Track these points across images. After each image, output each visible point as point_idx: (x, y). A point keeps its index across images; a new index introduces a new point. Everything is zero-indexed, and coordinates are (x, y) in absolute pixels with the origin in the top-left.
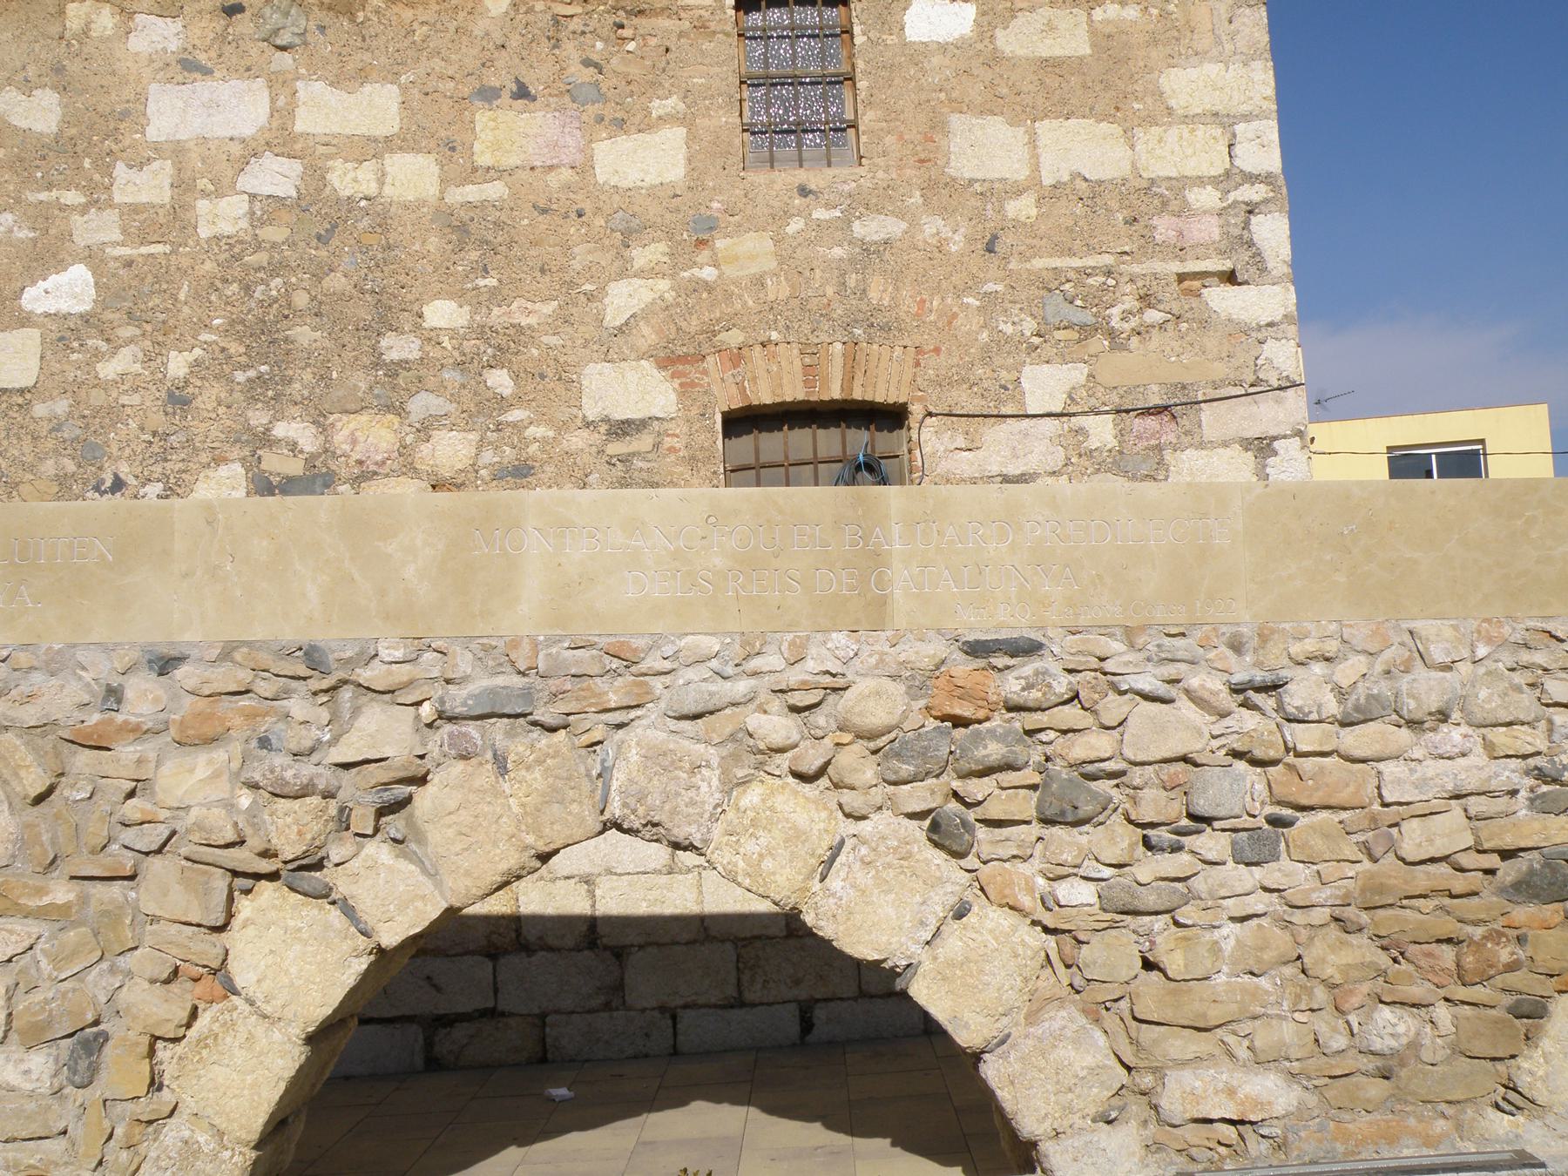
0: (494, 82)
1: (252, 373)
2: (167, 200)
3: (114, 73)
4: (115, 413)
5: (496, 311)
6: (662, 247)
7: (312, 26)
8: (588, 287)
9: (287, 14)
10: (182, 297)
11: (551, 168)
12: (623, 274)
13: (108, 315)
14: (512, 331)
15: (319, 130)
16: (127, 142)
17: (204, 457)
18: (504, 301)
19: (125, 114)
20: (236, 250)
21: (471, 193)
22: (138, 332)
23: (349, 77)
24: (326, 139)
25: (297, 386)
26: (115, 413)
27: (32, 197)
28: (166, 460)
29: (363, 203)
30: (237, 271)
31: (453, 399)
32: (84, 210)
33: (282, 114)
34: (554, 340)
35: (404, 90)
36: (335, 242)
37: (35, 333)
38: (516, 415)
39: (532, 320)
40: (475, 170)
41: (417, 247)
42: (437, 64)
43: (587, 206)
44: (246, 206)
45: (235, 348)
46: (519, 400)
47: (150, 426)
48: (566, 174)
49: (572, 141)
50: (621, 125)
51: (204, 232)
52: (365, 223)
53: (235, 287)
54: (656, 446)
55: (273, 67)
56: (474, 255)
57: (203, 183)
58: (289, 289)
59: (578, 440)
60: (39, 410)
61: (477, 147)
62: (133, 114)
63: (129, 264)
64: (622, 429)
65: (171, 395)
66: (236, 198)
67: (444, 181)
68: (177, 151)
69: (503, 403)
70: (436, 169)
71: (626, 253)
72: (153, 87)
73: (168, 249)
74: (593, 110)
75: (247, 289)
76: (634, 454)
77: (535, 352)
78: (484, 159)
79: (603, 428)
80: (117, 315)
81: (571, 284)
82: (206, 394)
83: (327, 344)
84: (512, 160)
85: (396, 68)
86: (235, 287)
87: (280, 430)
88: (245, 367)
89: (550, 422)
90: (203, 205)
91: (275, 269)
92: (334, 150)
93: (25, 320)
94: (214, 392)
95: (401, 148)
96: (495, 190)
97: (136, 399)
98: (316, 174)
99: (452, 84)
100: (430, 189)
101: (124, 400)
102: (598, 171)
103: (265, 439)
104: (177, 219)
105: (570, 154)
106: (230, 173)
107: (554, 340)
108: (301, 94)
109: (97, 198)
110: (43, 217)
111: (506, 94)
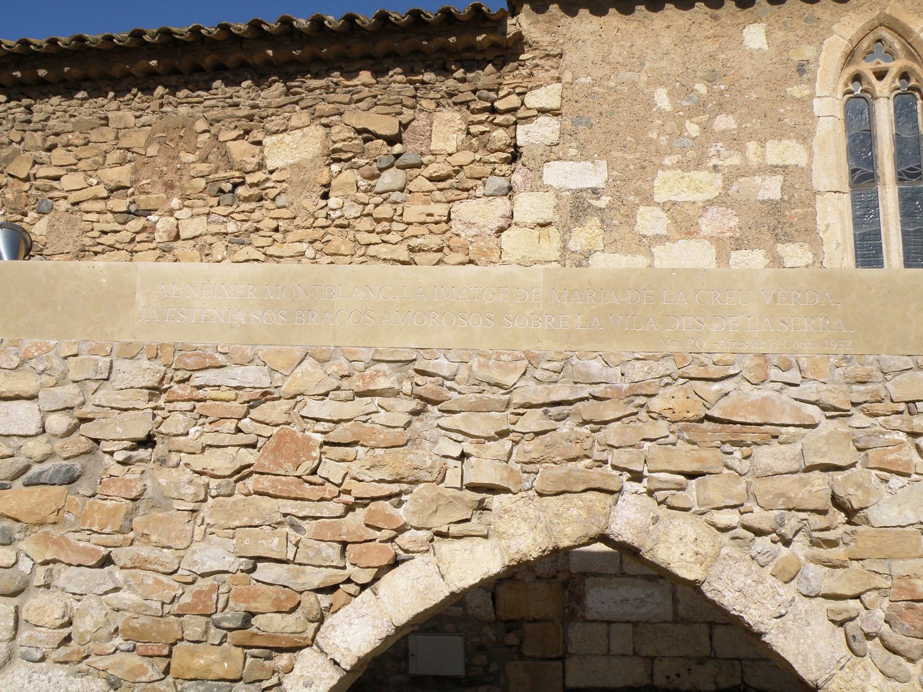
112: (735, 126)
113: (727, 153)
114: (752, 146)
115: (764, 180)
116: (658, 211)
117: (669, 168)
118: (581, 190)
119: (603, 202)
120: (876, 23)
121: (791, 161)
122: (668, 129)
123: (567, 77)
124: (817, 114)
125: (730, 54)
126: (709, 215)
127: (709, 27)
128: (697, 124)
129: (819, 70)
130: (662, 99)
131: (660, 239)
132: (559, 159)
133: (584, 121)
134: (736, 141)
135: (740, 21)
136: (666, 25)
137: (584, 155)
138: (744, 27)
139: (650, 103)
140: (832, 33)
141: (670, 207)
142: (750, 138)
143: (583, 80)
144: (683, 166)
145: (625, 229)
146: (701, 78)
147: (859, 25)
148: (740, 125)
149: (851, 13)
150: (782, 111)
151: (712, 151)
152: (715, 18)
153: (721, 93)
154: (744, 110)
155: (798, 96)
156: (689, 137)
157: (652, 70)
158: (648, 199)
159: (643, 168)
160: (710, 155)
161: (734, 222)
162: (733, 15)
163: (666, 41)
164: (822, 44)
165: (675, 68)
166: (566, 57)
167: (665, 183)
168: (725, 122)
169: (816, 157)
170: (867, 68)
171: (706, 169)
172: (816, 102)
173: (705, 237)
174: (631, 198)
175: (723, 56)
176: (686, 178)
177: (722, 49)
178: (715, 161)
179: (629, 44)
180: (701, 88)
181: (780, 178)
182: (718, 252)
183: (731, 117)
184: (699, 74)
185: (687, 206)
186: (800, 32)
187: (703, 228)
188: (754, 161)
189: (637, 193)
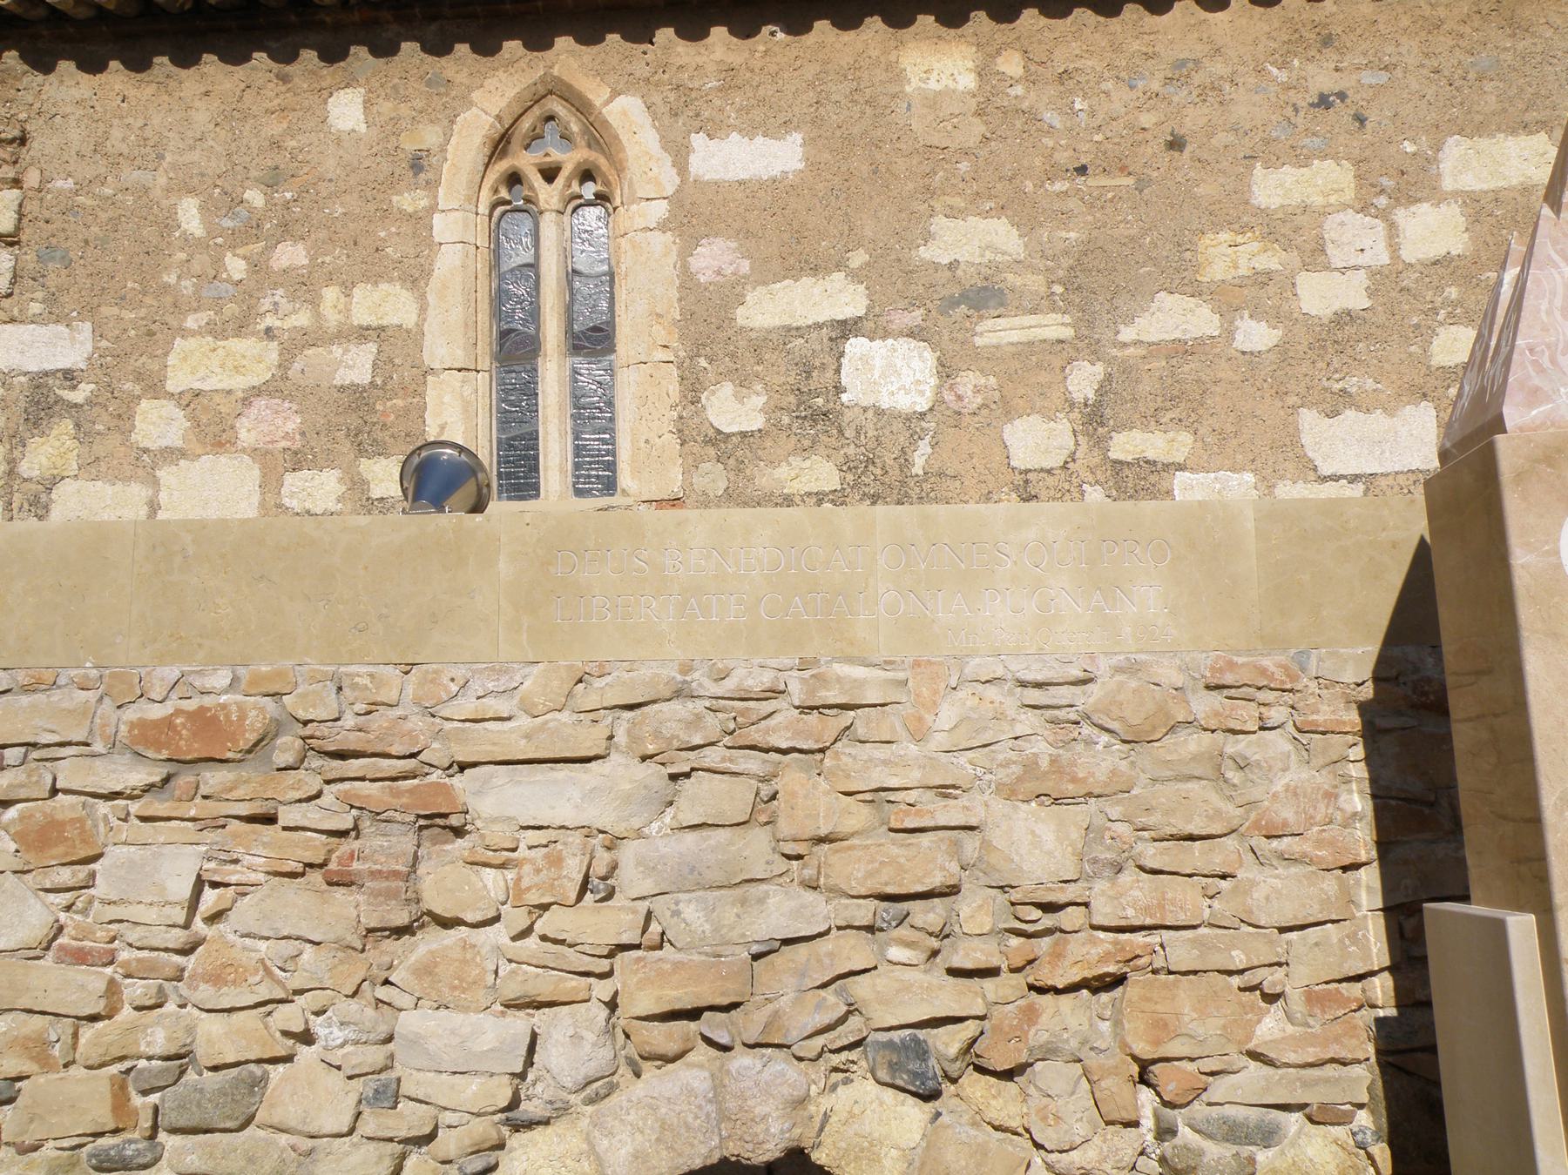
112: (305, 262)
113: (290, 307)
114: (331, 294)
115: (346, 351)
116: (169, 408)
117: (193, 333)
118: (46, 374)
119: (78, 396)
120: (542, 90)
121: (391, 319)
122: (196, 267)
123: (32, 178)
124: (437, 239)
125: (304, 139)
126: (253, 412)
127: (273, 93)
128: (245, 258)
129: (446, 166)
130: (190, 217)
131: (172, 455)
132: (13, 320)
133: (58, 254)
134: (304, 286)
135: (324, 84)
136: (203, 90)
137: (55, 314)
138: (331, 95)
139: (168, 224)
140: (472, 104)
141: (191, 400)
142: (329, 281)
143: (59, 184)
144: (216, 331)
145: (114, 440)
147: (511, 93)
148: (313, 259)
149: (500, 73)
150: (382, 234)
151: (266, 304)
152: (284, 79)
153: (287, 205)
154: (323, 234)
155: (410, 210)
157: (174, 166)
158: (155, 387)
159: (151, 334)
160: (262, 310)
161: (293, 424)
162: (313, 72)
163: (202, 117)
164: (452, 122)
165: (213, 164)
166: (35, 145)
167: (185, 359)
168: (291, 255)
169: (431, 312)
170: (526, 161)
171: (253, 334)
172: (437, 219)
173: (244, 450)
174: (128, 386)
175: (293, 143)
176: (220, 351)
177: (290, 132)
178: (269, 321)
179: (140, 123)
180: (255, 197)
181: (372, 347)
182: (264, 475)
183: (300, 246)
184: (254, 173)
185: (217, 399)
186: (419, 103)
187: (243, 434)
188: (332, 318)
189: (139, 377)
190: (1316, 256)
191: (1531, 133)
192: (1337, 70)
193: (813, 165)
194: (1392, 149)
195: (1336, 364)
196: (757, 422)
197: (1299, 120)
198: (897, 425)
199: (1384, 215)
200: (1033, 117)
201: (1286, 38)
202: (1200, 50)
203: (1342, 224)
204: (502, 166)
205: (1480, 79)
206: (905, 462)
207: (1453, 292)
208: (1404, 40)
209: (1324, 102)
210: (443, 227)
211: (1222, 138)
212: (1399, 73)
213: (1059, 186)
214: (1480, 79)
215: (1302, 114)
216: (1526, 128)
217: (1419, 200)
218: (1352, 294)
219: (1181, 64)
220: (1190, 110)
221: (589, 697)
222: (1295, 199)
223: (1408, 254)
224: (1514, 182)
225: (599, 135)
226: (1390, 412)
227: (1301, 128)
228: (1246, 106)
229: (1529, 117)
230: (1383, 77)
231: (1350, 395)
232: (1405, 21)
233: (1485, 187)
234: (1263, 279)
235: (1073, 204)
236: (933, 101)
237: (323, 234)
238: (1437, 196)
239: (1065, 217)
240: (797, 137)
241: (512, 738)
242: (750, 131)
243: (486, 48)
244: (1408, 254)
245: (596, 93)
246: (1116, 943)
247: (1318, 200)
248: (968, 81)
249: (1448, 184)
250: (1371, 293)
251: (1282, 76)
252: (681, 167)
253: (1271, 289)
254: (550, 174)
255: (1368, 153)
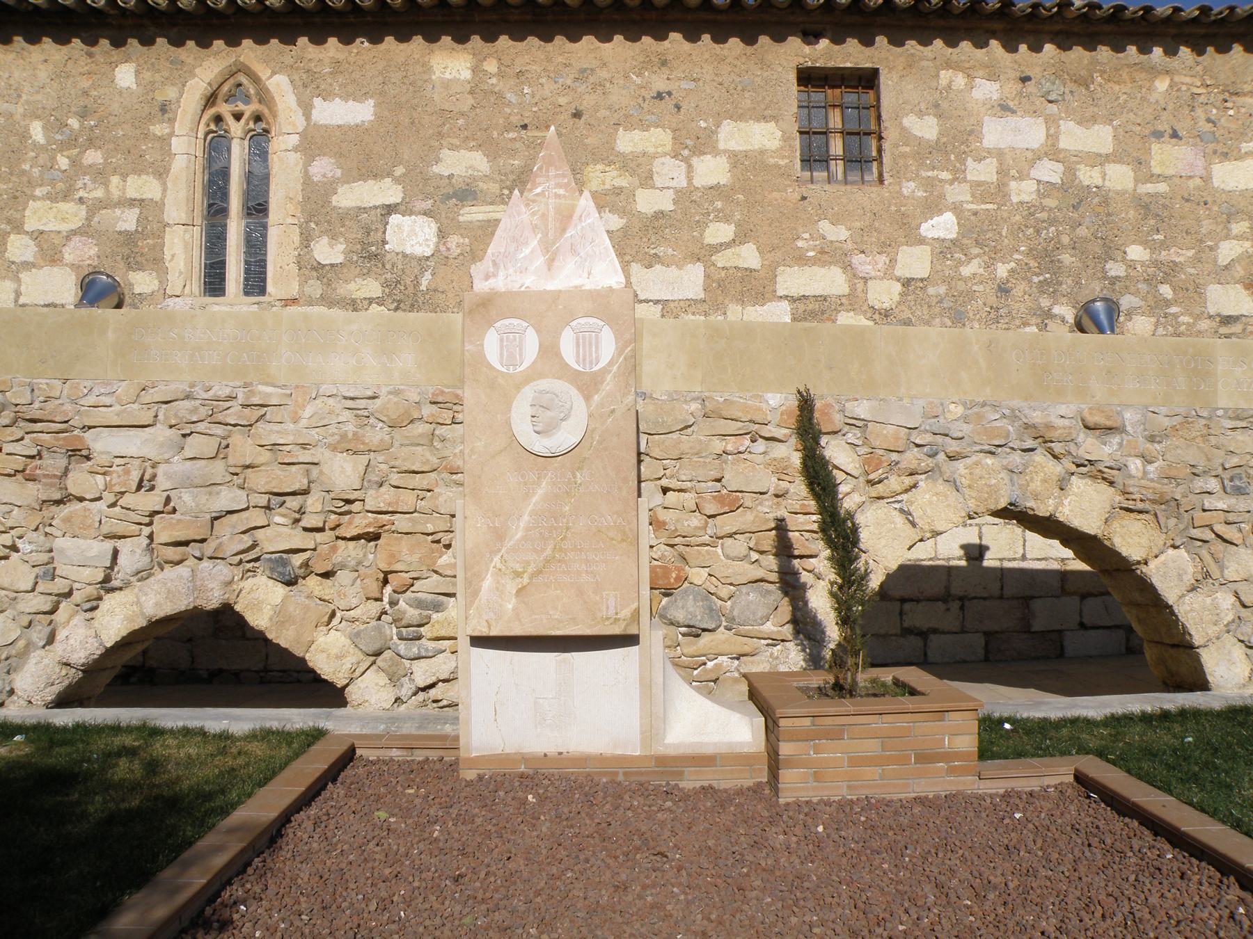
0: (1160, 128)
1: (1041, 278)
2: (995, 180)
3: (965, 109)
4: (970, 295)
5: (1164, 253)
6: (1247, 224)
7: (1067, 91)
8: (1209, 243)
9: (1054, 83)
10: (1004, 234)
11: (1190, 177)
12: (1227, 237)
13: (965, 241)
14: (1171, 264)
15: (1072, 148)
16: (973, 147)
17: (1018, 322)
18: (1168, 248)
19: (971, 132)
20: (1032, 210)
21: (1150, 188)
22: (982, 251)
23: (1087, 121)
24: (1075, 153)
25: (1064, 286)
26: (970, 295)
27: (924, 174)
28: (998, 322)
29: (1094, 190)
30: (1032, 221)
31: (1144, 299)
32: (951, 182)
33: (1053, 138)
34: (1192, 271)
35: (1115, 129)
36: (1081, 209)
37: (928, 248)
38: (1174, 310)
39: (1181, 259)
40: (1152, 176)
41: (1123, 215)
42: (1131, 116)
43: (1209, 200)
44: (1036, 187)
45: (1033, 264)
46: (1175, 302)
47: (989, 303)
48: (1198, 181)
49: (1200, 163)
50: (1225, 156)
51: (1015, 199)
52: (1096, 200)
53: (1031, 230)
54: (1244, 330)
55: (1047, 112)
56: (1152, 222)
57: (1013, 172)
58: (1059, 233)
59: (1204, 325)
60: (931, 291)
61: (1153, 163)
62: (974, 133)
63: (975, 214)
64: (1227, 320)
65: (999, 287)
66: (1030, 182)
67: (1137, 181)
68: (999, 154)
69: (1168, 303)
70: (1132, 174)
71: (1229, 225)
72: (986, 118)
73: (995, 207)
74: (1211, 146)
75: (1038, 232)
76: (1232, 334)
77: (1183, 276)
78: (1157, 170)
79: (1218, 319)
80: (970, 242)
81: (1201, 241)
82: (1018, 287)
83: (1079, 265)
84: (1170, 172)
85: (1111, 117)
86: (1031, 230)
87: (1057, 310)
88: (1037, 275)
89: (1191, 315)
90: (1013, 184)
91: (1052, 222)
92: (1080, 159)
93: (922, 241)
94: (1022, 287)
95: (1114, 161)
96: (1162, 187)
97: (981, 288)
98: (1070, 171)
99: (1140, 128)
100: (1131, 185)
101: (975, 288)
102: (1214, 180)
103: (1048, 314)
104: (999, 191)
105: (1200, 171)
106: (1027, 168)
107: (1192, 271)
108: (1062, 128)
109: (958, 176)
110: (930, 184)
111: (1167, 135)
112: (101, 161)
113: (92, 186)
114: (115, 180)
115: (123, 212)
116: (26, 240)
117: (39, 199)
120: (234, 69)
122: (41, 161)
124: (173, 152)
125: (102, 91)
126: (72, 244)
128: (68, 157)
129: (180, 111)
131: (27, 265)
134: (100, 175)
135: (113, 60)
138: (117, 66)
140: (195, 76)
141: (38, 235)
142: (115, 172)
146: (75, 113)
147: (217, 70)
148: (106, 160)
149: (211, 58)
150: (144, 147)
151: (80, 184)
152: (90, 55)
153: (91, 128)
154: (111, 146)
155: (159, 134)
156: (59, 170)
158: (18, 227)
159: (15, 198)
160: (77, 187)
161: (94, 251)
162: (106, 52)
164: (184, 86)
167: (35, 213)
168: (93, 157)
169: (169, 192)
170: (225, 109)
171: (73, 200)
172: (174, 139)
173: (66, 265)
175: (96, 93)
176: (54, 209)
177: (94, 86)
178: (82, 193)
180: (74, 123)
181: (137, 211)
183: (99, 152)
184: (73, 109)
185: (52, 236)
186: (166, 74)
187: (66, 256)
188: (116, 193)
189: (9, 221)
190: (647, 180)
191: (767, 122)
192: (668, 79)
193: (379, 118)
194: (694, 125)
195: (653, 239)
196: (339, 259)
197: (645, 106)
198: (414, 263)
199: (686, 160)
200: (500, 96)
201: (642, 60)
202: (595, 63)
203: (663, 164)
204: (211, 112)
205: (743, 90)
206: (417, 284)
207: (719, 204)
208: (705, 66)
209: (659, 96)
210: (178, 145)
211: (603, 113)
212: (701, 83)
213: (511, 135)
214: (743, 90)
215: (647, 102)
216: (765, 119)
217: (705, 153)
218: (665, 202)
219: (582, 71)
220: (587, 96)
221: (146, 397)
222: (639, 149)
223: (697, 182)
224: (756, 147)
225: (264, 97)
226: (680, 267)
227: (646, 110)
228: (618, 96)
229: (766, 113)
230: (692, 85)
231: (659, 257)
232: (706, 56)
233: (741, 148)
234: (618, 191)
235: (518, 145)
236: (446, 84)
237: (111, 146)
238: (716, 152)
239: (513, 153)
240: (371, 102)
241: (110, 416)
242: (345, 98)
243: (204, 44)
244: (697, 182)
245: (263, 72)
246: (375, 518)
247: (651, 150)
248: (467, 74)
249: (721, 146)
250: (675, 202)
251: (638, 81)
252: (308, 116)
253: (622, 197)
254: (238, 117)
255: (680, 126)
